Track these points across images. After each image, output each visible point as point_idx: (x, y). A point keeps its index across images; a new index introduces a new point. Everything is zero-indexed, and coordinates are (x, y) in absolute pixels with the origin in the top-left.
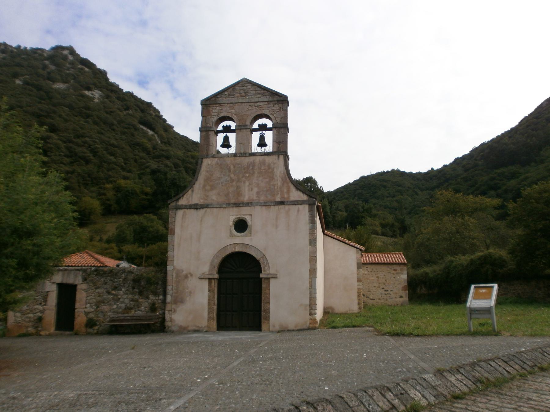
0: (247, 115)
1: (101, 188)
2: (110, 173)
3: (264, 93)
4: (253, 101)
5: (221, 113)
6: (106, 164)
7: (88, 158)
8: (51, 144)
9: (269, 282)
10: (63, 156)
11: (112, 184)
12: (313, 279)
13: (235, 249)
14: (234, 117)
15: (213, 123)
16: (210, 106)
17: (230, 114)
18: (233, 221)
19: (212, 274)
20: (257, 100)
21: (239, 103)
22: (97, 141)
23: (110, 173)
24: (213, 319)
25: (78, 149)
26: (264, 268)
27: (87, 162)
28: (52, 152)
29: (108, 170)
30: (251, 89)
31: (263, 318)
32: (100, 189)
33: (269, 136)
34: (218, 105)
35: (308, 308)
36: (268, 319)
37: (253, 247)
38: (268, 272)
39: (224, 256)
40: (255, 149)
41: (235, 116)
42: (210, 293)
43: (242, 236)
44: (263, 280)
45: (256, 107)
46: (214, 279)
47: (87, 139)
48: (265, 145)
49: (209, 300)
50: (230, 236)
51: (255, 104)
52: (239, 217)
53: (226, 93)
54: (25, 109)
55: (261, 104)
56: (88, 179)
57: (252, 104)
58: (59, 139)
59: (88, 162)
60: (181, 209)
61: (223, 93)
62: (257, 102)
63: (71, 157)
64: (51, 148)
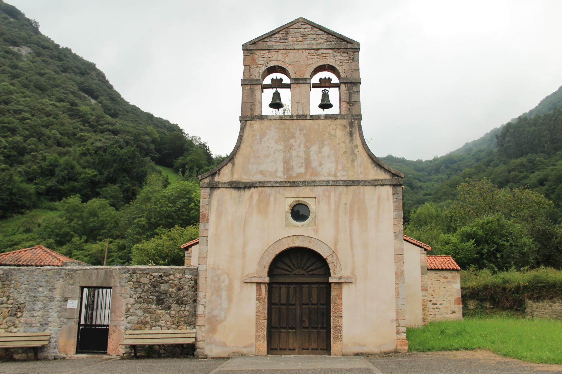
0: (306, 65)
3: (327, 38)
4: (314, 48)
5: (270, 61)
9: (341, 288)
12: (400, 284)
13: (293, 243)
14: (289, 69)
15: (259, 75)
16: (256, 52)
17: (283, 63)
18: (290, 206)
19: (261, 277)
20: (319, 47)
21: (294, 49)
24: (264, 339)
26: (334, 270)
30: (311, 32)
31: (333, 338)
33: (334, 94)
34: (265, 52)
35: (395, 324)
36: (339, 338)
37: (318, 241)
38: (338, 275)
39: (277, 253)
40: (315, 110)
41: (290, 67)
42: (259, 302)
43: (303, 226)
44: (332, 285)
45: (318, 55)
46: (264, 283)
48: (329, 106)
49: (257, 312)
50: (286, 226)
51: (316, 52)
52: (298, 201)
53: (277, 36)
55: (325, 51)
57: (313, 51)
60: (219, 188)
61: (273, 36)
62: (318, 49)
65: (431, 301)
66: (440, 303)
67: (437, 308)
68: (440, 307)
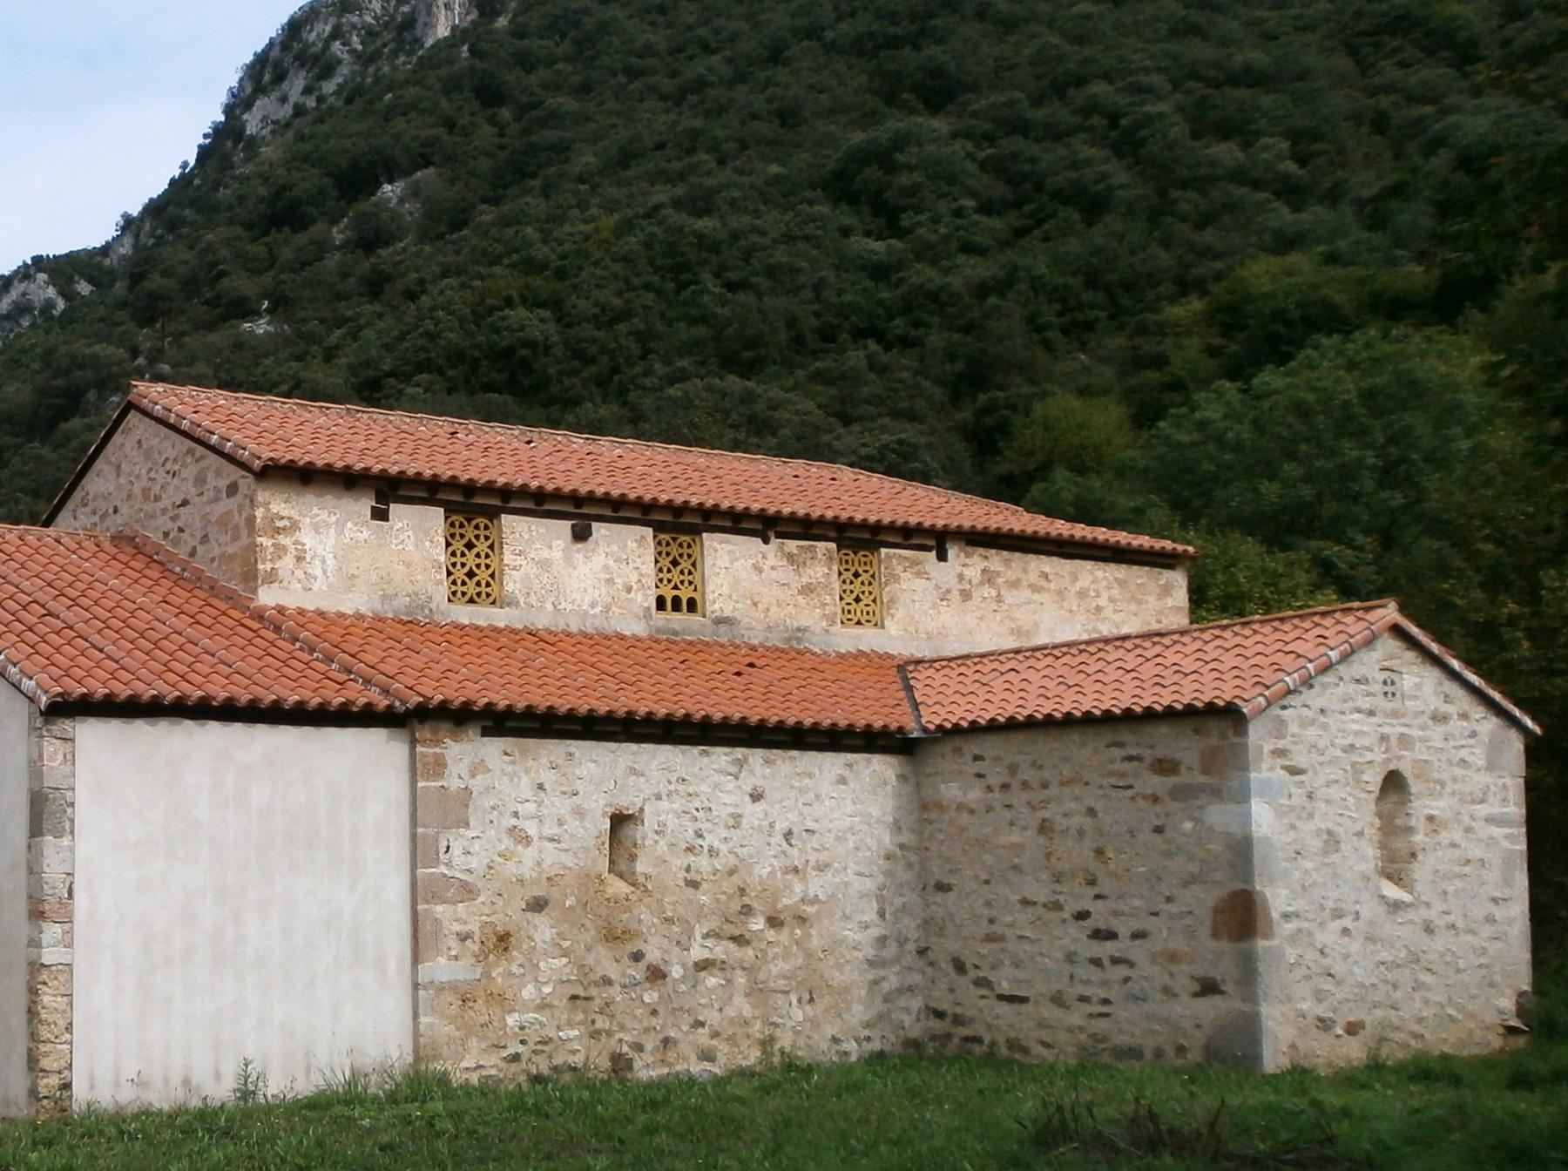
1: (1142, 330)
2: (1208, 237)
6: (1192, 194)
7: (1100, 187)
8: (910, 168)
10: (977, 211)
11: (1204, 293)
22: (1155, 79)
23: (1208, 237)
25: (1049, 156)
27: (1094, 206)
28: (918, 211)
29: (1200, 226)
32: (1138, 340)
47: (1098, 88)
54: (829, 35)
56: (1087, 296)
58: (954, 136)
59: (1094, 206)
63: (1019, 204)
64: (913, 190)
65: (1082, 916)
66: (1136, 925)
67: (1115, 961)
68: (1137, 951)
